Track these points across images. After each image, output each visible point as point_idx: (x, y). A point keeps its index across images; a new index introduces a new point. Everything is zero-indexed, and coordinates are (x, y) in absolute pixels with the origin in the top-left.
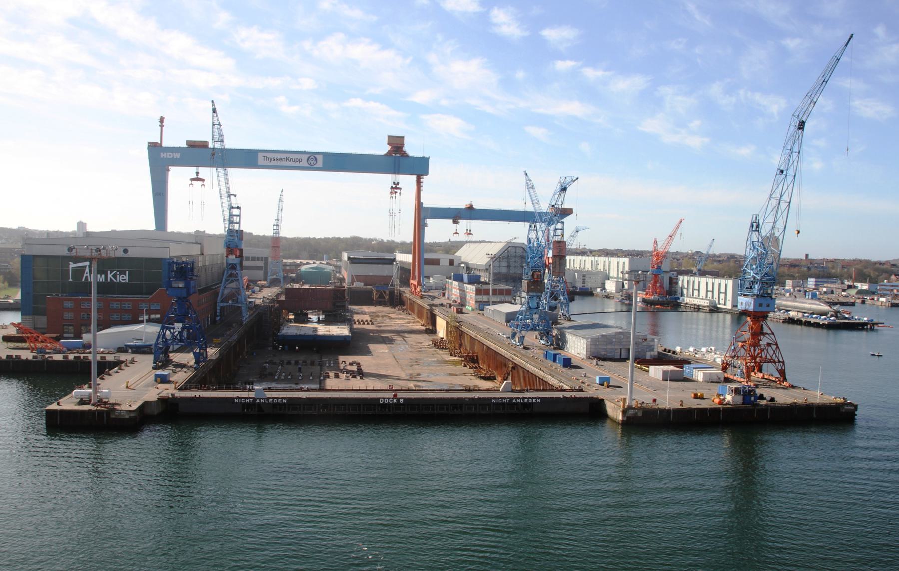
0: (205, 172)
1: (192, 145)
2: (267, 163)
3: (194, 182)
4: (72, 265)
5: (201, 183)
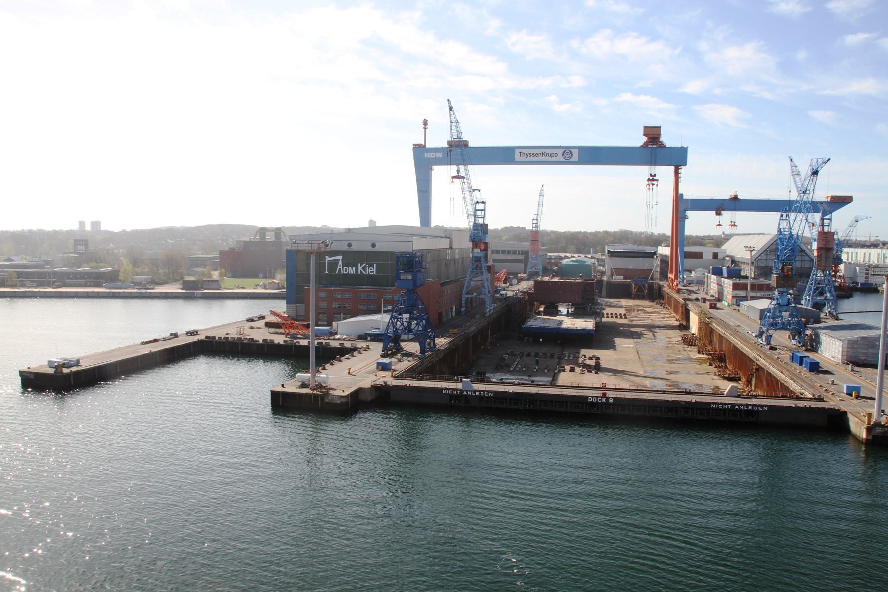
2: (524, 159)
3: (455, 180)
4: (328, 259)
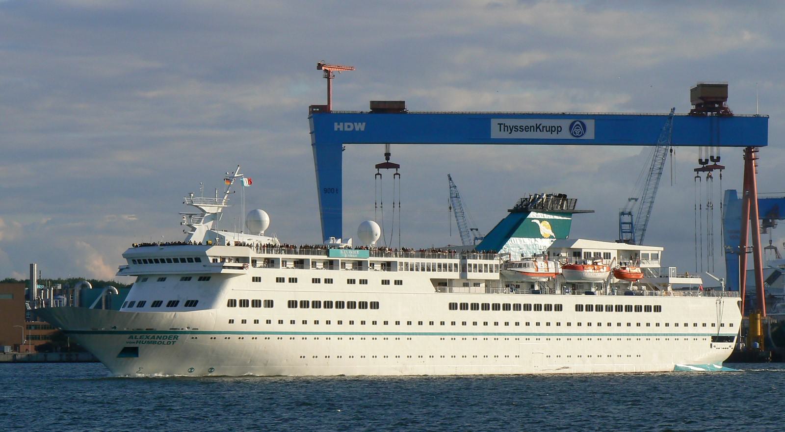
0: (399, 151)
1: (378, 108)
3: (382, 171)
5: (394, 171)
